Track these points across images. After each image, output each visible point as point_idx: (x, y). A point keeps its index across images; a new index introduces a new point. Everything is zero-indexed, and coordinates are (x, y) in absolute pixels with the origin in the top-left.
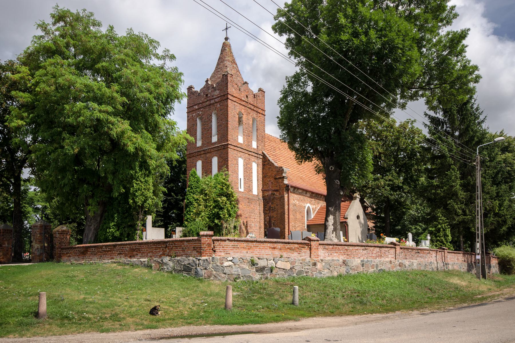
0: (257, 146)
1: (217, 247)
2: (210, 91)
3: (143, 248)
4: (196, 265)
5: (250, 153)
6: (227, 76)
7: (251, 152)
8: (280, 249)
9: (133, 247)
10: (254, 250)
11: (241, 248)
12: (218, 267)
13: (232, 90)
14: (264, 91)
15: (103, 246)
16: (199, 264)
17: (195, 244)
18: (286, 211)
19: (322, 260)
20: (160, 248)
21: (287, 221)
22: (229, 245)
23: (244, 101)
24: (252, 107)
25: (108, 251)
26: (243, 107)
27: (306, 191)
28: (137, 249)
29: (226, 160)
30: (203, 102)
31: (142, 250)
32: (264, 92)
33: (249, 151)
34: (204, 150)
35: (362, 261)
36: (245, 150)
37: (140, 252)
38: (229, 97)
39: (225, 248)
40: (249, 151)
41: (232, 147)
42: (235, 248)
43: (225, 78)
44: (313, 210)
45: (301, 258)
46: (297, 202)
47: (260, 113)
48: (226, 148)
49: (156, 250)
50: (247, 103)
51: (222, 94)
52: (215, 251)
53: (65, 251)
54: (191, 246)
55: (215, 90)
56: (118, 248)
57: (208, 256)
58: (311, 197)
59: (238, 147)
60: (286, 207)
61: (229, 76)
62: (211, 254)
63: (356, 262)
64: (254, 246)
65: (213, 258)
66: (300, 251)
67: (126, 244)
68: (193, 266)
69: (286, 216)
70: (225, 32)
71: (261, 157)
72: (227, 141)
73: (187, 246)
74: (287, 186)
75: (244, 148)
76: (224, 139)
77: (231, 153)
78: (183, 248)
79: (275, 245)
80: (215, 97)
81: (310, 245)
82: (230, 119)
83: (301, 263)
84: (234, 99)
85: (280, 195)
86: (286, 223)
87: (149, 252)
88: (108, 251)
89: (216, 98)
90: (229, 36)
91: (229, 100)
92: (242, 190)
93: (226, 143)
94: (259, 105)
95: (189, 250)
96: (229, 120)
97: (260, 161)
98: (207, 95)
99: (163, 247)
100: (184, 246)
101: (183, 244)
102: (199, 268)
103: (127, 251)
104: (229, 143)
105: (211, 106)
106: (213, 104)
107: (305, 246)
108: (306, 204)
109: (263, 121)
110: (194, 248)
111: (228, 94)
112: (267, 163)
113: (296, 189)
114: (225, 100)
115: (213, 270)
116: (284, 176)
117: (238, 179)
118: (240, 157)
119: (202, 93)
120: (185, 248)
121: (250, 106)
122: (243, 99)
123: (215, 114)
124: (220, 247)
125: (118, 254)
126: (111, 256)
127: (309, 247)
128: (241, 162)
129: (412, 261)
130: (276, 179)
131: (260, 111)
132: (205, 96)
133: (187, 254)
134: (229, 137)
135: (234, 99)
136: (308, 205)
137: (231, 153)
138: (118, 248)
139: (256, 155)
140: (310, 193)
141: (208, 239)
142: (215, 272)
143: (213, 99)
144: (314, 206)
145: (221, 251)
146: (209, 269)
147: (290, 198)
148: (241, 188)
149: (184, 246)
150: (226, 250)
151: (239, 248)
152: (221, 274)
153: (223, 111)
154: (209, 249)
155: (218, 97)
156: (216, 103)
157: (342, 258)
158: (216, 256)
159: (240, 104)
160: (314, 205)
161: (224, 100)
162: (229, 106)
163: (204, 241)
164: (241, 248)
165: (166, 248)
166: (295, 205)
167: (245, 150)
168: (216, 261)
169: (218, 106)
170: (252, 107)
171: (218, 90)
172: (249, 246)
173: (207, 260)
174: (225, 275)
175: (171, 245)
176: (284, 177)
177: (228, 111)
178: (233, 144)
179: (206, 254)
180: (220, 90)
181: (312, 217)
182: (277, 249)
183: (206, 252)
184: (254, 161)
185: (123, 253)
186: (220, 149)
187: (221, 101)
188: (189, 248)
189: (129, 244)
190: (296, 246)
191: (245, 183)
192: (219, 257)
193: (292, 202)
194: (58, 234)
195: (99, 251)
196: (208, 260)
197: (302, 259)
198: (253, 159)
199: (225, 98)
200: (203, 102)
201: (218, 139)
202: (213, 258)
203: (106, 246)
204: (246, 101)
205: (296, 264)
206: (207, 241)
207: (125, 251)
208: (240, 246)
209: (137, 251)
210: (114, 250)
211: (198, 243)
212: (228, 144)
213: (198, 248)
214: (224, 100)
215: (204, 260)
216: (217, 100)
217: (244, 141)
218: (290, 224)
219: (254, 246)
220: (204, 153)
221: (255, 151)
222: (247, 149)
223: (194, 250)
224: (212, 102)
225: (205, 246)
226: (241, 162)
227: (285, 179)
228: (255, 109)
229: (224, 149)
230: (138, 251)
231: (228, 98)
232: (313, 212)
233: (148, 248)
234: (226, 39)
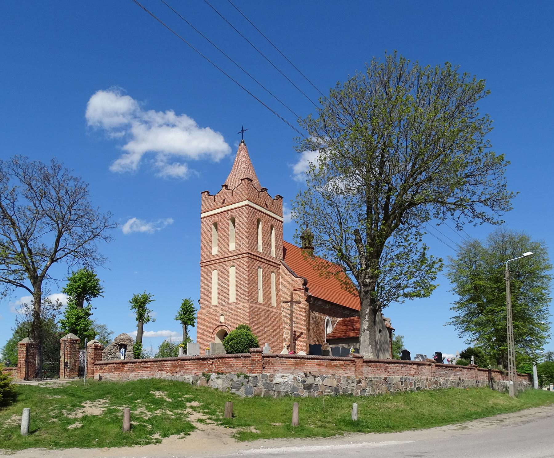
1: (266, 364)
8: (327, 366)
11: (289, 365)
19: (366, 378)
20: (205, 364)
25: (147, 367)
28: (180, 365)
31: (186, 367)
35: (401, 379)
42: (283, 364)
53: (99, 367)
54: (240, 362)
63: (396, 379)
66: (345, 369)
70: (241, 134)
73: (236, 363)
78: (231, 365)
87: (194, 369)
88: (147, 367)
95: (238, 367)
99: (209, 364)
101: (232, 361)
103: (169, 367)
110: (243, 364)
120: (233, 365)
124: (269, 364)
125: (159, 370)
129: (446, 378)
141: (258, 355)
145: (270, 368)
151: (287, 365)
157: (383, 376)
164: (289, 365)
175: (218, 361)
179: (256, 371)
185: (165, 370)
188: (238, 365)
190: (342, 362)
195: (137, 367)
196: (258, 377)
197: (347, 376)
205: (342, 382)
206: (257, 357)
207: (166, 367)
211: (248, 360)
223: (243, 367)
225: (255, 363)
233: (192, 364)
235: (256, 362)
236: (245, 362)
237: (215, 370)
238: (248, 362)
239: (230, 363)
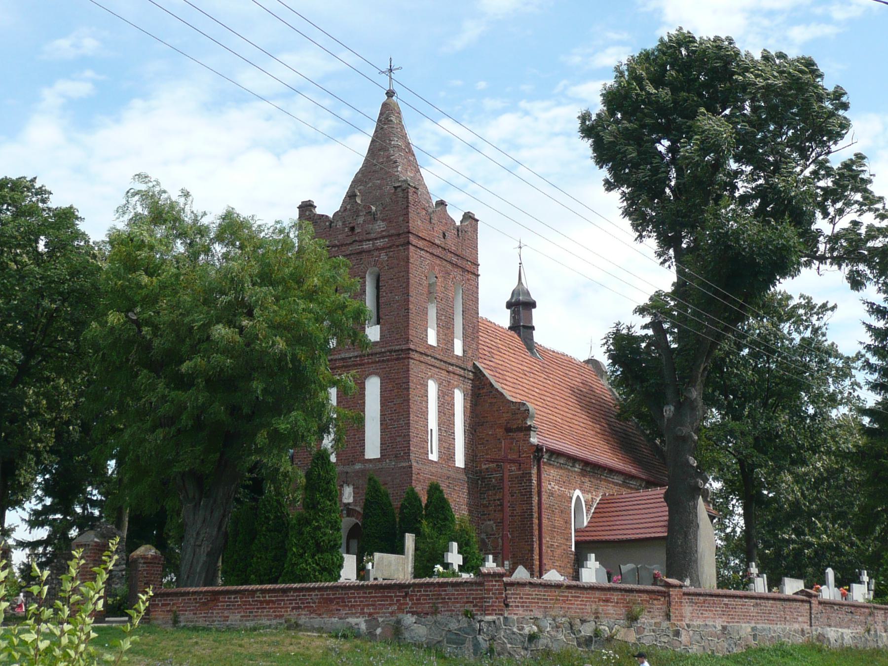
0: (464, 351)
1: (511, 598)
2: (361, 220)
3: (351, 598)
4: (474, 630)
5: (451, 368)
6: (405, 191)
7: (452, 365)
8: (617, 603)
9: (333, 595)
10: (572, 604)
12: (514, 636)
13: (417, 223)
14: (476, 217)
15: (257, 590)
16: (480, 630)
17: (470, 590)
18: (535, 509)
19: (688, 626)
21: (536, 533)
22: (530, 595)
23: (438, 246)
24: (454, 259)
25: (268, 602)
26: (438, 262)
27: (573, 459)
28: (339, 598)
29: (404, 386)
30: (342, 245)
31: (351, 602)
32: (477, 221)
33: (449, 364)
34: (343, 359)
35: (753, 629)
36: (441, 361)
37: (347, 606)
38: (412, 238)
39: (524, 600)
40: (449, 364)
41: (416, 356)
42: (540, 599)
43: (401, 194)
44: (586, 505)
45: (653, 621)
46: (556, 487)
47: (468, 271)
48: (405, 358)
49: (381, 601)
50: (445, 249)
51: (393, 232)
52: (507, 605)
53: (161, 601)
54: (461, 594)
55: (375, 219)
56: (292, 596)
57: (496, 614)
58: (583, 473)
59: (428, 356)
60: (535, 499)
61: (411, 190)
62: (502, 610)
63: (746, 629)
64: (572, 597)
65: (506, 619)
67: (314, 589)
68: (468, 634)
69: (536, 521)
71: (471, 375)
72: (407, 341)
73: (453, 594)
74: (538, 449)
75: (439, 357)
76: (397, 336)
77: (415, 369)
79: (608, 595)
80: (373, 236)
81: (669, 596)
82: (413, 292)
83: (654, 631)
84: (421, 244)
85: (519, 469)
86: (535, 539)
87: (368, 605)
88: (268, 602)
89: (376, 239)
90: (396, 87)
91: (410, 246)
92: (434, 457)
93: (404, 347)
94: (467, 253)
95: (458, 602)
96: (411, 294)
97: (469, 385)
98: (352, 229)
99: (400, 596)
100: (447, 595)
102: (481, 637)
103: (314, 603)
104: (412, 347)
105: (364, 256)
106: (369, 251)
107: (659, 597)
108: (572, 491)
109: (474, 289)
111: (409, 232)
112: (485, 391)
113: (554, 456)
114: (402, 245)
115: (506, 641)
116: (530, 426)
117: (427, 431)
118: (431, 377)
119: (340, 223)
121: (449, 256)
122: (437, 242)
123: (371, 274)
124: (516, 598)
125: (293, 608)
126: (274, 612)
127: (667, 599)
128: (432, 388)
129: (840, 630)
130: (508, 430)
131: (468, 266)
132: (347, 230)
133: (454, 611)
134: (410, 332)
135: (421, 244)
136: (578, 493)
137: (415, 369)
138: (292, 596)
139: (462, 372)
140: (582, 464)
141: (496, 581)
142: (509, 646)
143: (369, 240)
144: (589, 496)
145: (518, 606)
146: (500, 639)
147: (544, 476)
148: (432, 453)
149: (447, 595)
150: (526, 602)
151: (547, 599)
152: (519, 650)
153: (396, 270)
154: (499, 602)
155: (383, 237)
156: (377, 249)
157: (719, 623)
158: (509, 614)
159: (431, 253)
160: (589, 492)
161: (398, 246)
162: (411, 260)
163: (489, 586)
165: (405, 597)
166: (552, 494)
167: (441, 361)
168: (511, 625)
169: (383, 257)
170: (454, 259)
171: (383, 220)
172: (565, 596)
173: (494, 622)
174: (526, 652)
175: (418, 591)
176: (529, 428)
177: (408, 272)
178: (418, 349)
179: (493, 610)
180: (387, 220)
181: (585, 524)
182: (612, 602)
183: (493, 606)
184: (457, 387)
185: (305, 607)
186: (388, 360)
187: (390, 247)
189: (320, 589)
190: (645, 596)
191: (440, 440)
192: (515, 617)
193: (547, 486)
194: (144, 563)
195: (245, 601)
196: (497, 622)
197: (655, 623)
198: (455, 380)
199: (402, 240)
200: (342, 245)
201: (382, 336)
202: (506, 619)
203: (263, 591)
204: (443, 246)
206: (495, 585)
207: (309, 603)
208: (549, 596)
209: (338, 603)
210: (283, 600)
211: (477, 590)
212: (410, 349)
213: (476, 599)
214: (398, 246)
215: (489, 622)
216: (380, 243)
217: (438, 341)
218: (544, 541)
219: (572, 597)
220: (342, 367)
221: (460, 363)
222: (445, 359)
223: (467, 602)
224: (366, 246)
225: (491, 595)
226: (432, 388)
227: (532, 432)
228: (460, 262)
229: (397, 359)
230: (342, 602)
231: (409, 243)
232: (588, 511)
233: (364, 597)
234: (390, 94)
235: (493, 594)
236: (473, 594)
237: (410, 608)
238: (477, 594)
239: (441, 595)
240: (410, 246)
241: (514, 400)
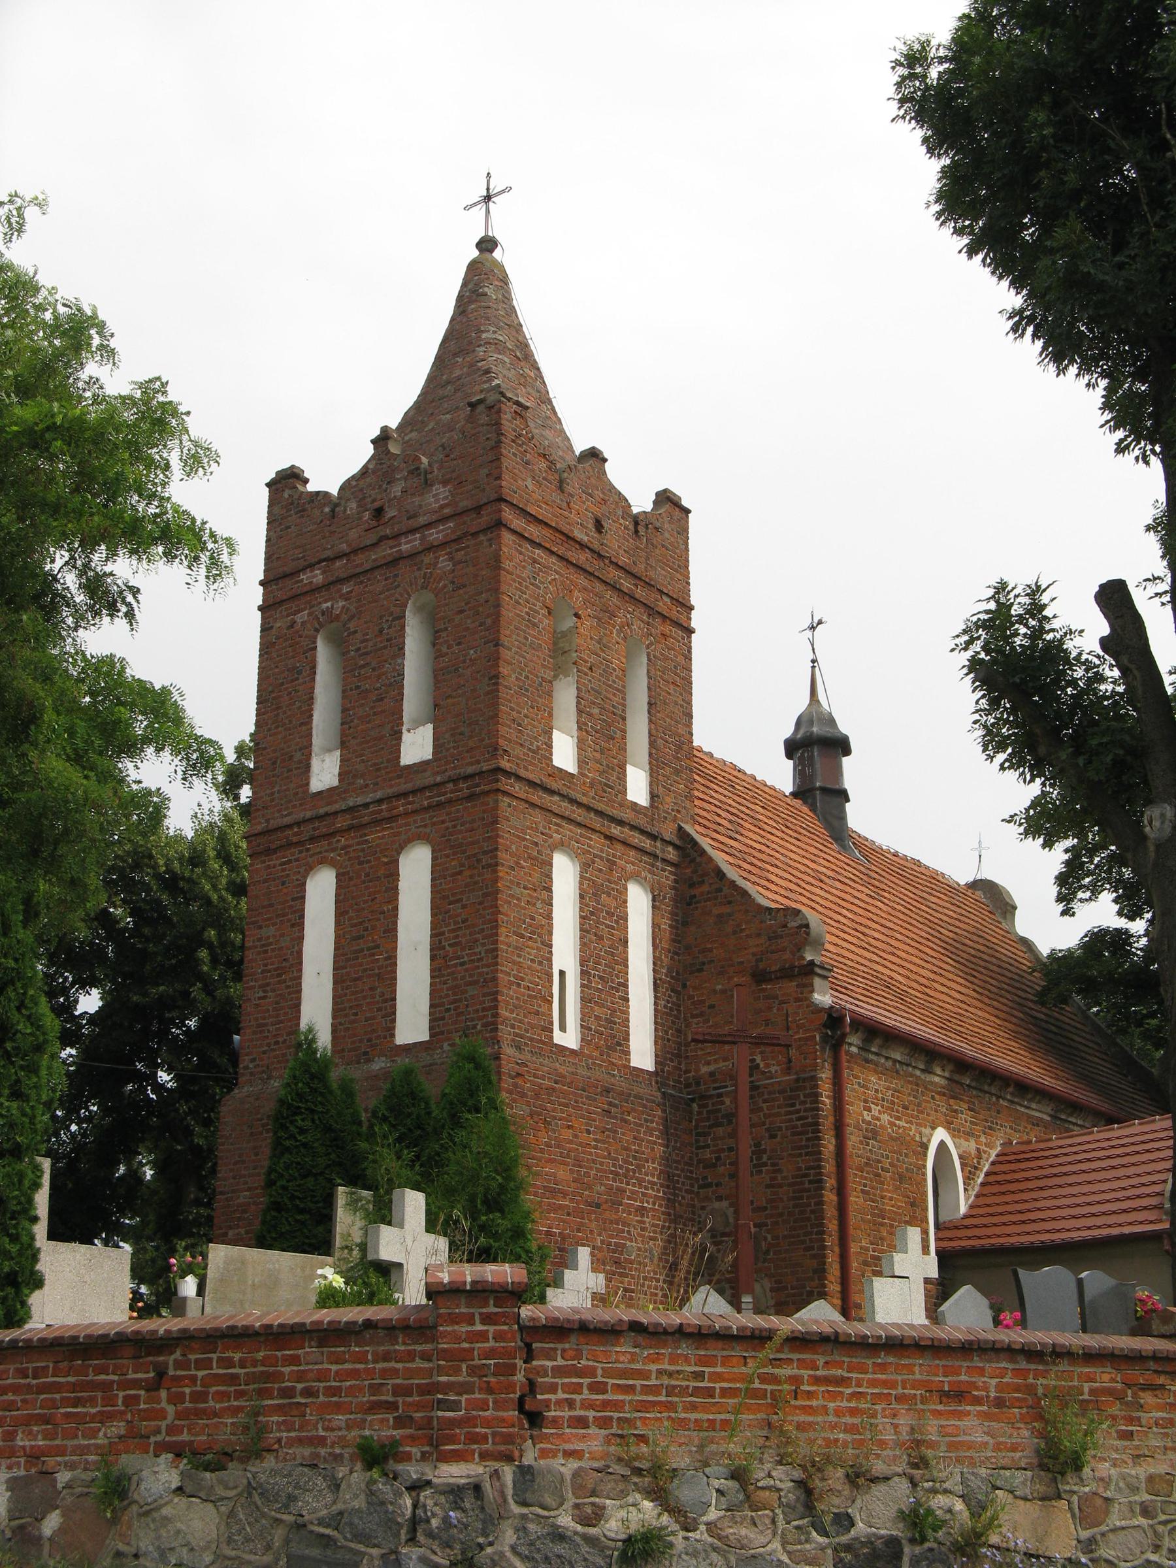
1: (553, 1389)
2: (397, 490)
4: (390, 1523)
5: (616, 831)
6: (494, 409)
7: (620, 823)
8: (999, 1403)
11: (725, 1392)
12: (560, 1549)
16: (414, 1522)
17: (386, 1357)
18: (829, 1167)
21: (832, 1226)
23: (583, 546)
24: (626, 584)
26: (582, 580)
27: (928, 1053)
29: (485, 860)
30: (355, 552)
34: (350, 810)
36: (589, 808)
38: (508, 514)
39: (609, 1396)
41: (518, 789)
43: (484, 419)
44: (963, 1165)
45: (1140, 1472)
46: (885, 1118)
47: (664, 617)
48: (486, 793)
49: (76, 1402)
51: (465, 504)
52: (535, 1419)
54: (354, 1374)
55: (428, 484)
57: (484, 1456)
58: (953, 1092)
59: (552, 792)
60: (828, 1143)
61: (508, 410)
64: (817, 1380)
65: (526, 1474)
66: (1130, 1420)
69: (830, 1197)
70: (479, 211)
71: (671, 854)
72: (495, 750)
73: (322, 1376)
74: (833, 1019)
75: (584, 800)
76: (471, 744)
78: (288, 1393)
80: (422, 520)
82: (510, 637)
83: (1146, 1512)
84: (533, 531)
85: (788, 1070)
86: (831, 1241)
87: (27, 1421)
89: (428, 526)
90: (497, 233)
92: (569, 1038)
94: (659, 575)
95: (338, 1408)
96: (505, 641)
97: (667, 878)
98: (379, 512)
99: (135, 1384)
101: (295, 1360)
102: (415, 1553)
104: (504, 764)
107: (1162, 1380)
108: (927, 1131)
109: (681, 659)
110: (375, 1389)
111: (501, 500)
112: (705, 888)
113: (878, 1041)
114: (484, 531)
116: (812, 963)
118: (561, 846)
119: (353, 505)
120: (308, 1393)
121: (612, 574)
123: (420, 609)
124: (577, 1389)
130: (760, 977)
131: (664, 604)
133: (322, 1441)
134: (503, 730)
135: (533, 531)
136: (940, 1134)
139: (647, 844)
140: (950, 1067)
141: (487, 1319)
143: (413, 531)
144: (971, 1146)
145: (582, 1422)
147: (851, 1090)
148: (563, 1028)
149: (300, 1377)
150: (617, 1406)
151: (710, 1393)
154: (498, 1406)
155: (444, 519)
156: (431, 548)
158: (544, 1454)
159: (561, 558)
160: (969, 1135)
161: (475, 535)
162: (507, 564)
164: (725, 1392)
165: (153, 1387)
166: (872, 1133)
167: (589, 808)
168: (549, 1500)
169: (444, 563)
170: (626, 584)
171: (445, 483)
173: (477, 1488)
175: (200, 1365)
176: (810, 969)
179: (473, 1439)
181: (963, 1209)
182: (977, 1401)
184: (635, 877)
186: (450, 801)
187: (457, 540)
188: (335, 1391)
190: (1106, 1377)
191: (585, 1000)
193: (856, 1112)
196: (487, 1486)
197: (1151, 1479)
198: (628, 861)
199: (485, 519)
200: (355, 552)
202: (526, 1474)
205: (1115, 1521)
206: (483, 1336)
211: (410, 1356)
212: (499, 770)
213: (406, 1391)
214: (475, 535)
215: (455, 1493)
216: (435, 535)
217: (582, 762)
218: (854, 1248)
219: (817, 1380)
220: (350, 828)
221: (642, 821)
222: (601, 806)
223: (374, 1407)
227: (817, 982)
228: (640, 593)
229: (471, 797)
231: (499, 524)
232: (968, 1180)
235: (472, 1370)
236: (395, 1373)
237: (171, 1430)
238: (410, 1373)
239: (277, 1377)
240: (507, 537)
241: (765, 903)
